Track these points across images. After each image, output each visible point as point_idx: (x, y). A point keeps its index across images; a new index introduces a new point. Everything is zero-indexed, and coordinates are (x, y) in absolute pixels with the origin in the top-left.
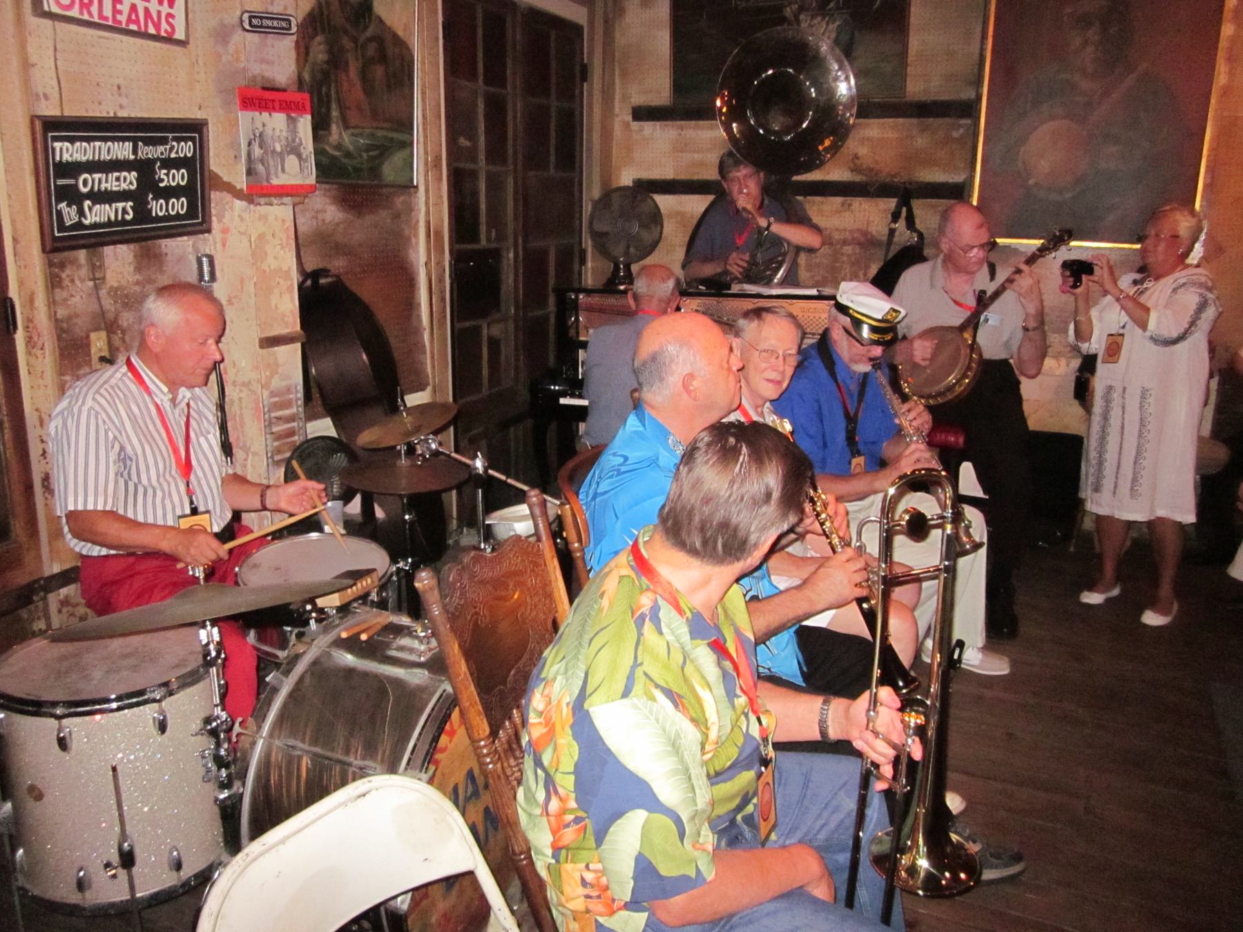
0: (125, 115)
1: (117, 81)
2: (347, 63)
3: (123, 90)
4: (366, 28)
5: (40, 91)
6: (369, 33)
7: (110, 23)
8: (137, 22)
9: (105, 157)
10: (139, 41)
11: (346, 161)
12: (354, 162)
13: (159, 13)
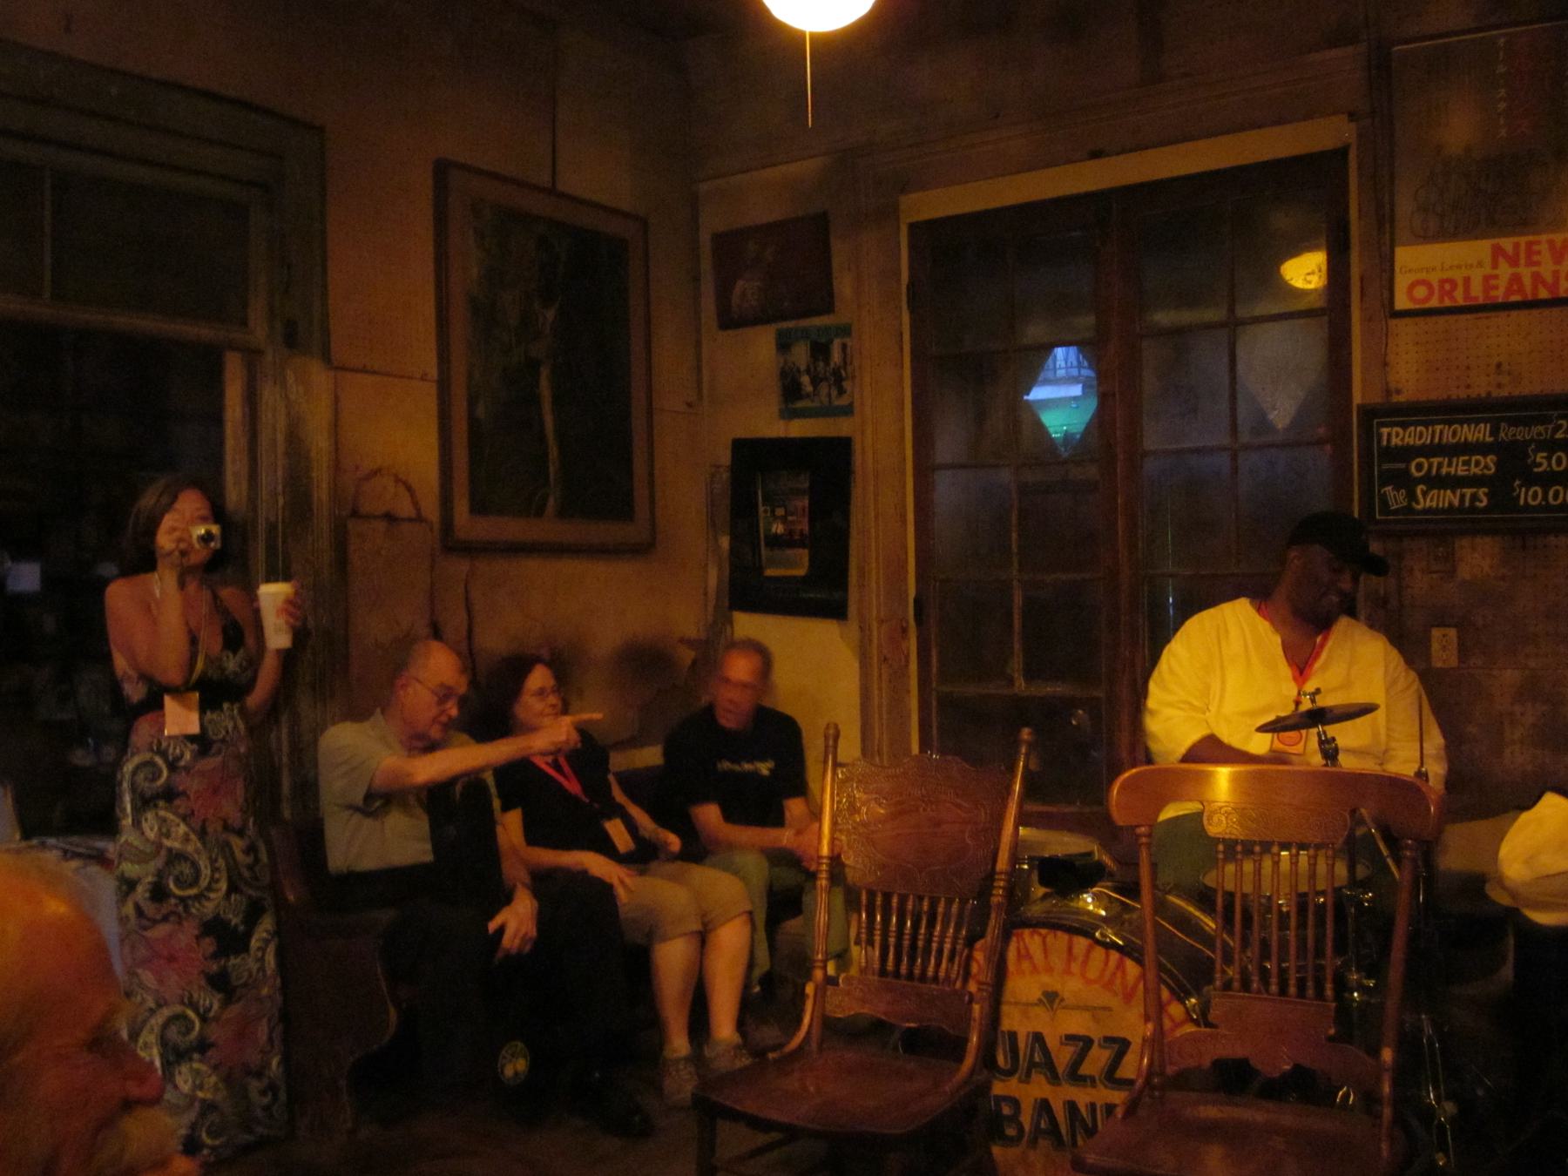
0: (1504, 393)
1: (1496, 360)
3: (1505, 367)
5: (1393, 386)
7: (1481, 301)
8: (1521, 290)
9: (1448, 438)
10: (1535, 312)
13: (1556, 274)
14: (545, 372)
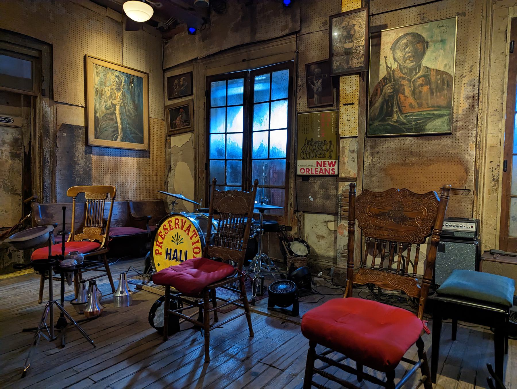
2: (404, 90)
4: (416, 73)
6: (419, 75)
11: (401, 127)
12: (407, 126)
14: (117, 108)
